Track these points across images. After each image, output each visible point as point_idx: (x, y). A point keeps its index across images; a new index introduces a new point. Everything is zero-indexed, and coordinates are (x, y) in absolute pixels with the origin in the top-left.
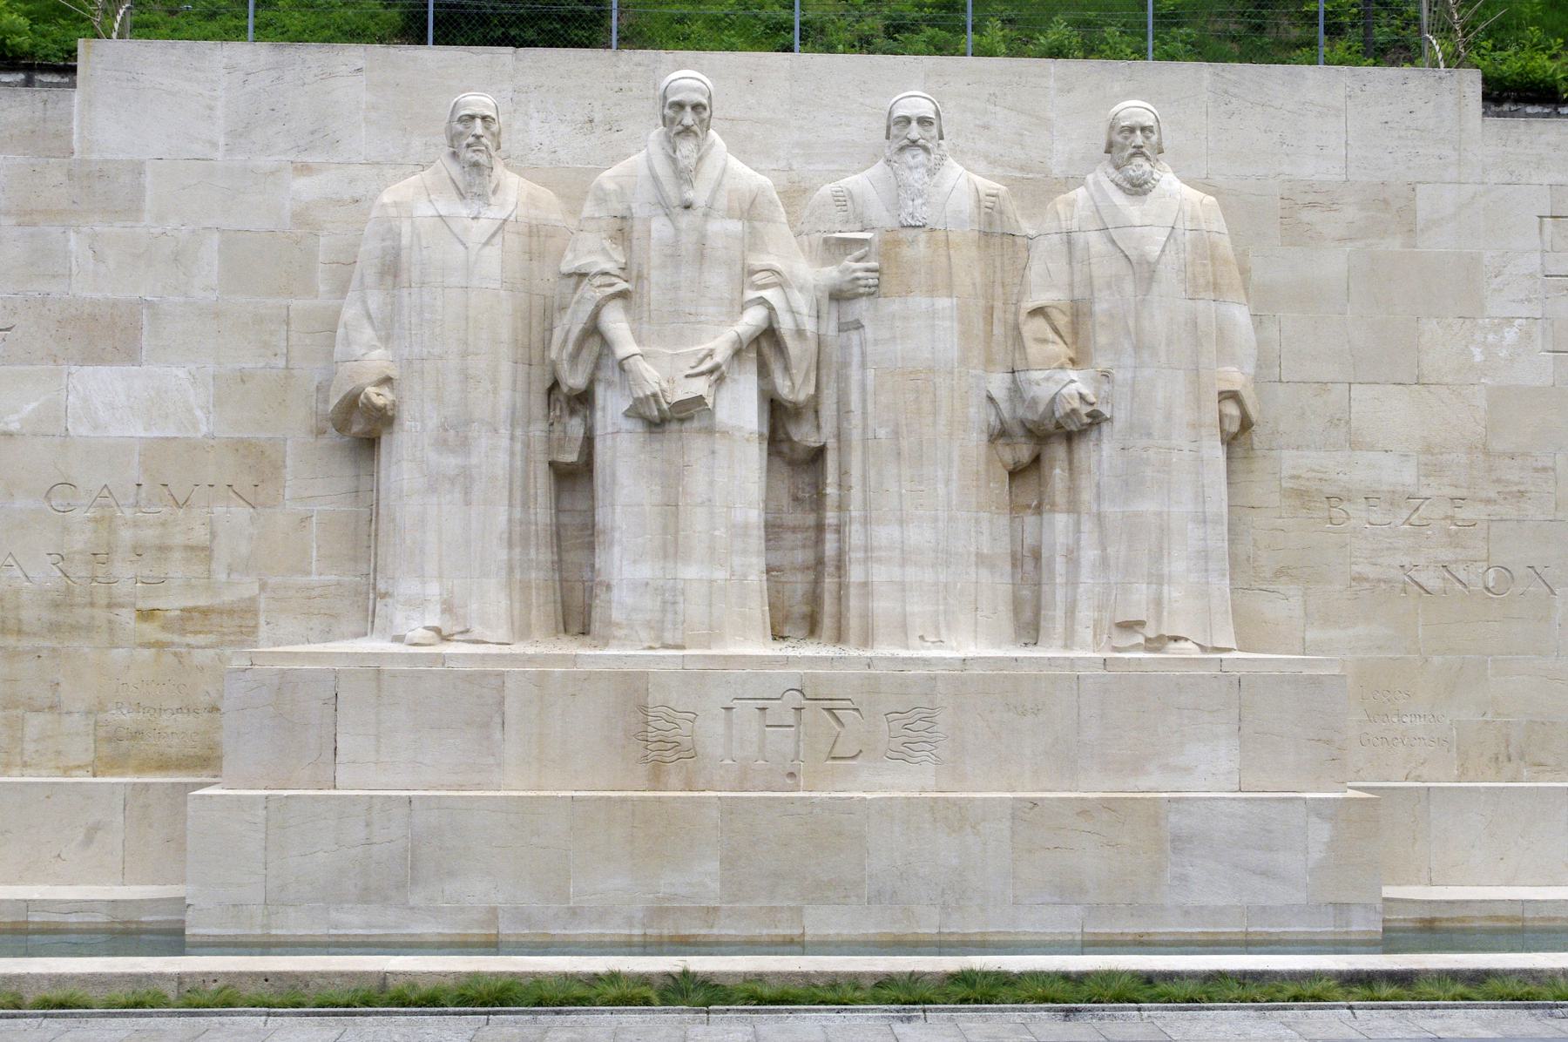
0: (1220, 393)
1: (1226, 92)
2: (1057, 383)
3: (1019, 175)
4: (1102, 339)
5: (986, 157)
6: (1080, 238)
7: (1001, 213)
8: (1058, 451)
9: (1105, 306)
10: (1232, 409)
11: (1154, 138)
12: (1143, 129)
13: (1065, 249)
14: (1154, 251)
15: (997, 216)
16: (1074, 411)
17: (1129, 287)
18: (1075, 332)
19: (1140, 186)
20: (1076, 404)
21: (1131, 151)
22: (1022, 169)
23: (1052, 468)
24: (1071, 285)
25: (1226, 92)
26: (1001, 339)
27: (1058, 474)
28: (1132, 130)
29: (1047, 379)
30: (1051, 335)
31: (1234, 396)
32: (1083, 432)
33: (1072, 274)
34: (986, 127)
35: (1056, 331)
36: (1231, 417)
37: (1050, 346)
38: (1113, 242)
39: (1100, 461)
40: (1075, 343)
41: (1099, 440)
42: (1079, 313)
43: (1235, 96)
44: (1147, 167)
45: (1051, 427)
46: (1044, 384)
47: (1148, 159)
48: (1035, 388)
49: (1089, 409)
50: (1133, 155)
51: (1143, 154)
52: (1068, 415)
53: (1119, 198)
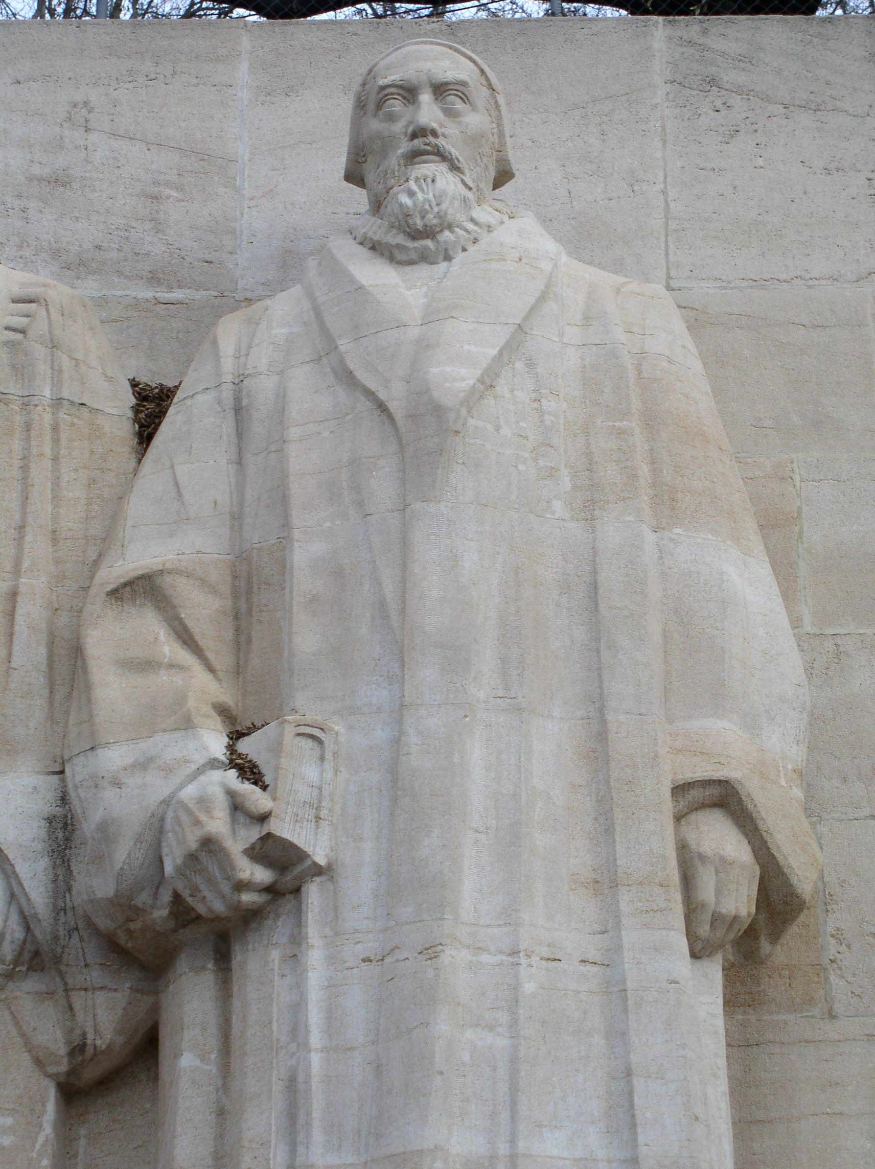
0: (680, 790)
1: (713, 82)
2: (168, 770)
3: (146, 293)
4: (307, 638)
5: (56, 253)
6: (264, 389)
7: (54, 345)
8: (191, 1000)
9: (318, 548)
10: (718, 837)
11: (475, 120)
12: (440, 90)
13: (228, 426)
14: (453, 375)
15: (40, 352)
16: (209, 844)
17: (383, 487)
18: (241, 642)
19: (428, 233)
20: (218, 823)
21: (405, 147)
22: (154, 279)
23: (177, 1056)
24: (237, 518)
25: (713, 82)
26: (38, 680)
27: (188, 1062)
28: (409, 93)
29: (143, 765)
30: (170, 649)
31: (724, 798)
32: (249, 919)
33: (240, 488)
34: (60, 181)
35: (186, 638)
36: (723, 864)
37: (164, 677)
38: (348, 378)
39: (298, 1007)
40: (238, 670)
41: (298, 940)
42: (252, 587)
43: (739, 90)
44: (447, 182)
45: (161, 913)
46: (132, 781)
47: (455, 168)
48: (109, 794)
49: (254, 834)
50: (414, 157)
51: (441, 155)
52: (192, 857)
53: (374, 275)
